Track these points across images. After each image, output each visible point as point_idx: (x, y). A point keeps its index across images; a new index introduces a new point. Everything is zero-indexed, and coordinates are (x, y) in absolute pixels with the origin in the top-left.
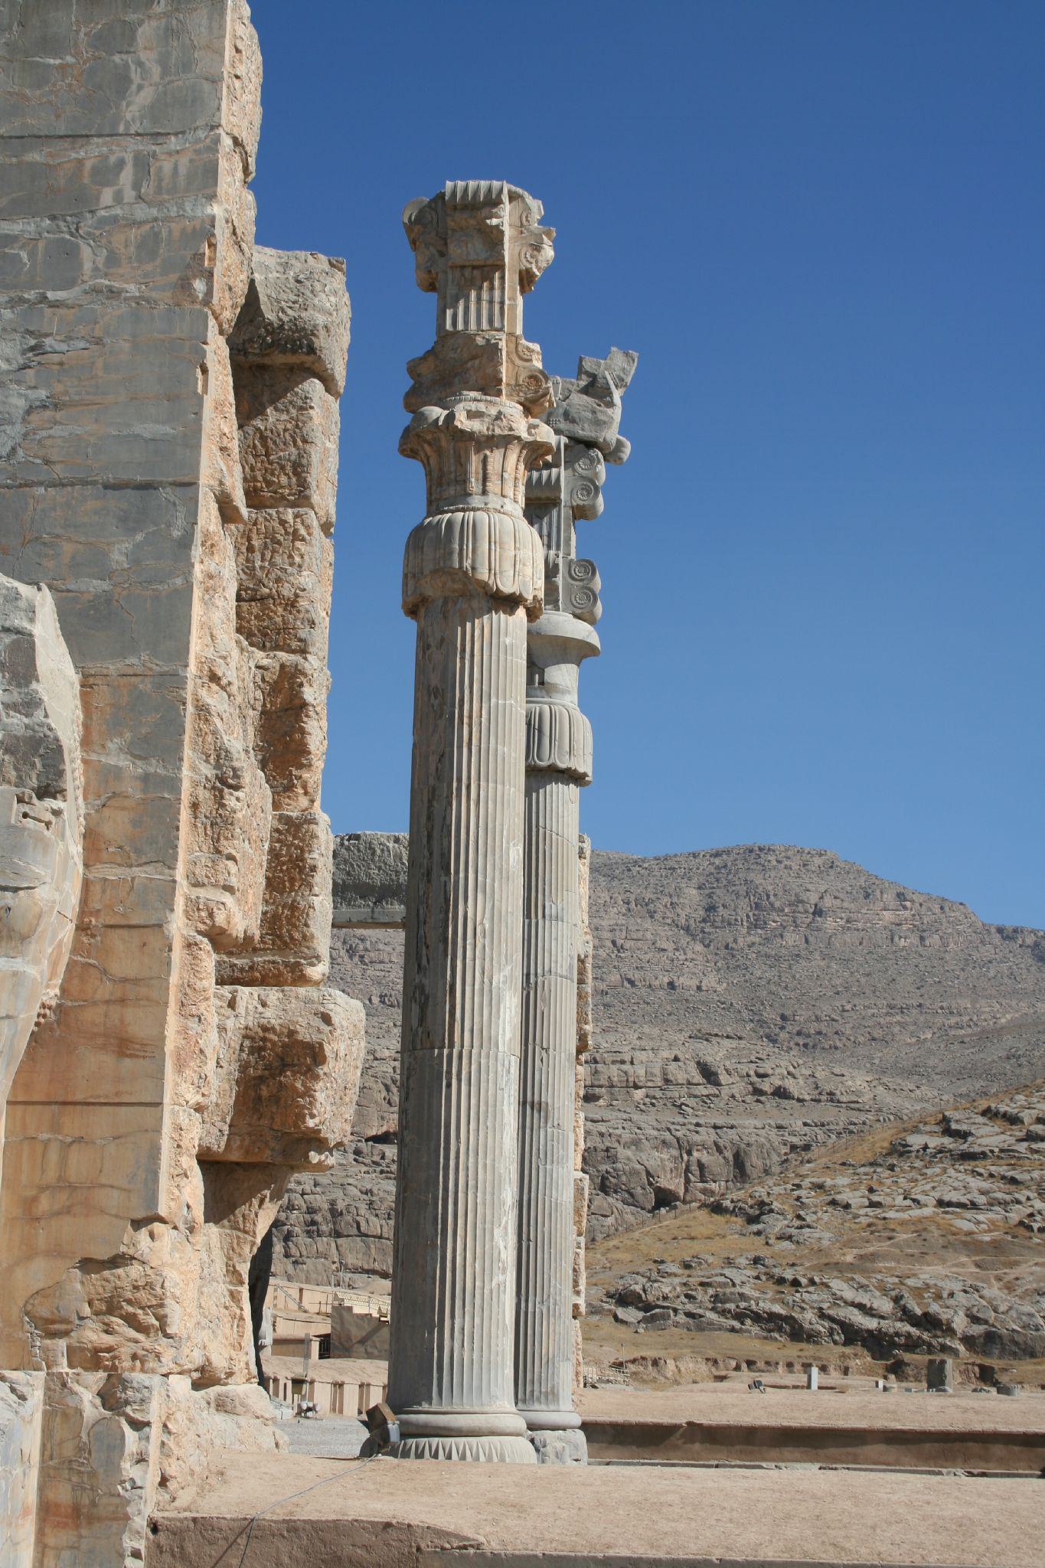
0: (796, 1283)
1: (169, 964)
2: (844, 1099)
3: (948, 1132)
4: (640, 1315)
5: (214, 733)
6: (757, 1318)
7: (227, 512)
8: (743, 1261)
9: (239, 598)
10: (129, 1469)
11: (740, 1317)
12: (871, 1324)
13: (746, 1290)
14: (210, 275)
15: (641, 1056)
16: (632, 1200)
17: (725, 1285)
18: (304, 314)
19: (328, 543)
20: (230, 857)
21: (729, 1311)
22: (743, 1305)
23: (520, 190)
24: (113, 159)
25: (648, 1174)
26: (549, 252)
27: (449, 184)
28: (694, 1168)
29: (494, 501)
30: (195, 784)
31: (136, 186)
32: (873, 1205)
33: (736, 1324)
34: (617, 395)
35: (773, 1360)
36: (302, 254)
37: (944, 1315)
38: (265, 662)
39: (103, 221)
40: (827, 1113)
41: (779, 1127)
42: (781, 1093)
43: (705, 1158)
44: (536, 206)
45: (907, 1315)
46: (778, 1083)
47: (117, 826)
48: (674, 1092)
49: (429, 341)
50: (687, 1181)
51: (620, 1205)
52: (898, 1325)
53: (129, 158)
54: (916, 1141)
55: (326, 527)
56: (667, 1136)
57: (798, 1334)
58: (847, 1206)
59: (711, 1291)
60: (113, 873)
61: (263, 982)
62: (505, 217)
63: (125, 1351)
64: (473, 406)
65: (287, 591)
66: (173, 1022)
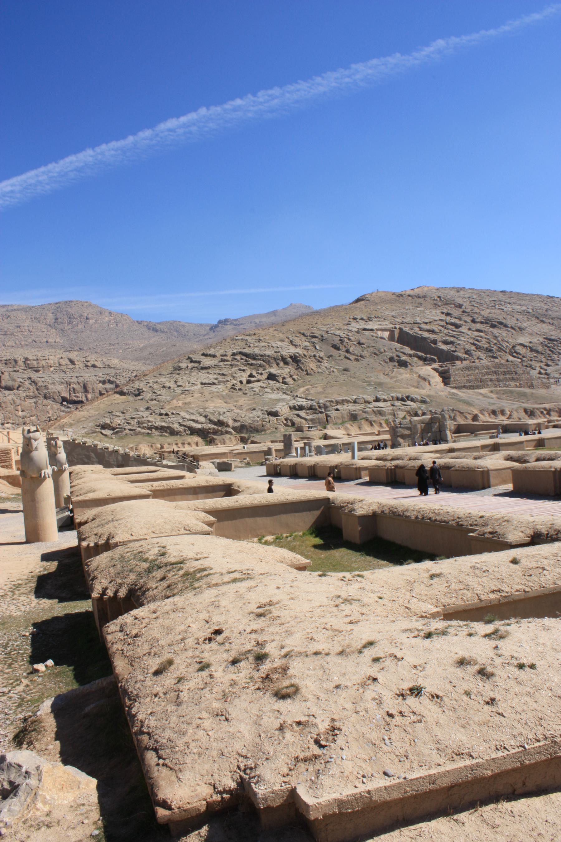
3: (192, 361)
4: (111, 432)
6: (156, 428)
11: (150, 428)
12: (199, 426)
13: (150, 419)
15: (51, 357)
16: (55, 400)
17: (139, 418)
21: (145, 427)
22: (150, 424)
25: (59, 392)
28: (72, 390)
33: (150, 432)
35: (171, 443)
37: (225, 420)
40: (108, 371)
41: (95, 376)
42: (94, 366)
43: (75, 386)
45: (211, 421)
46: (93, 363)
48: (62, 368)
50: (70, 394)
51: (51, 402)
52: (209, 425)
54: (183, 365)
56: (63, 380)
57: (173, 433)
58: (169, 388)
59: (136, 420)
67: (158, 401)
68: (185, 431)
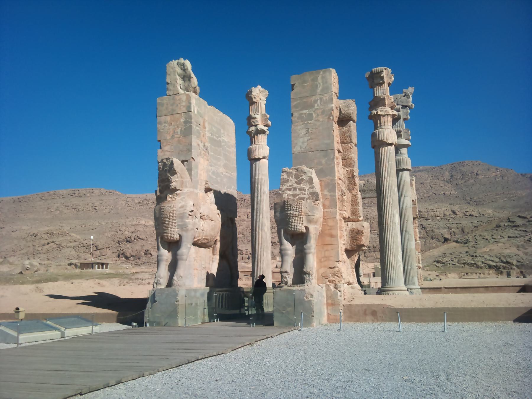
0: (476, 256)
1: (337, 223)
2: (486, 215)
4: (442, 265)
5: (341, 187)
6: (468, 264)
7: (339, 152)
8: (463, 252)
9: (342, 159)
10: (339, 298)
11: (464, 264)
12: (494, 264)
14: (333, 116)
15: (438, 210)
16: (439, 240)
18: (349, 111)
19: (356, 148)
20: (345, 206)
23: (386, 68)
24: (316, 99)
25: (442, 234)
26: (393, 79)
27: (373, 69)
28: (453, 233)
29: (386, 127)
30: (338, 195)
31: (320, 103)
32: (493, 238)
33: (464, 266)
34: (411, 97)
36: (348, 100)
38: (347, 170)
39: (316, 109)
40: (482, 219)
41: (471, 223)
42: (471, 215)
44: (390, 70)
46: (470, 213)
47: (327, 203)
48: (446, 217)
49: (372, 98)
51: (436, 242)
53: (319, 98)
55: (355, 145)
57: (478, 267)
58: (487, 239)
59: (457, 259)
60: (327, 210)
61: (352, 221)
62: (384, 74)
63: (337, 281)
64: (381, 110)
65: (350, 158)
66: (339, 232)
67: (476, 248)
68: (485, 266)
